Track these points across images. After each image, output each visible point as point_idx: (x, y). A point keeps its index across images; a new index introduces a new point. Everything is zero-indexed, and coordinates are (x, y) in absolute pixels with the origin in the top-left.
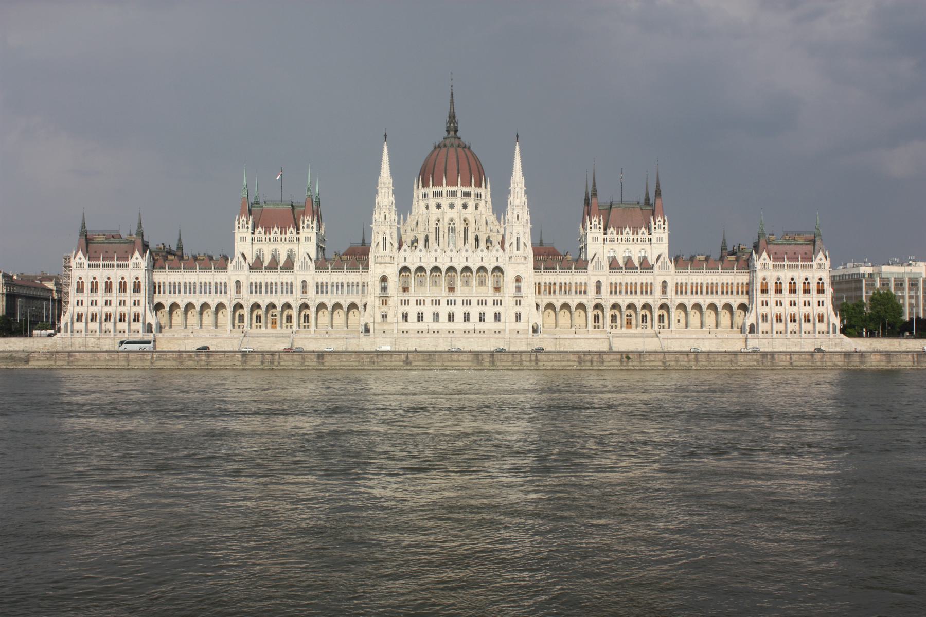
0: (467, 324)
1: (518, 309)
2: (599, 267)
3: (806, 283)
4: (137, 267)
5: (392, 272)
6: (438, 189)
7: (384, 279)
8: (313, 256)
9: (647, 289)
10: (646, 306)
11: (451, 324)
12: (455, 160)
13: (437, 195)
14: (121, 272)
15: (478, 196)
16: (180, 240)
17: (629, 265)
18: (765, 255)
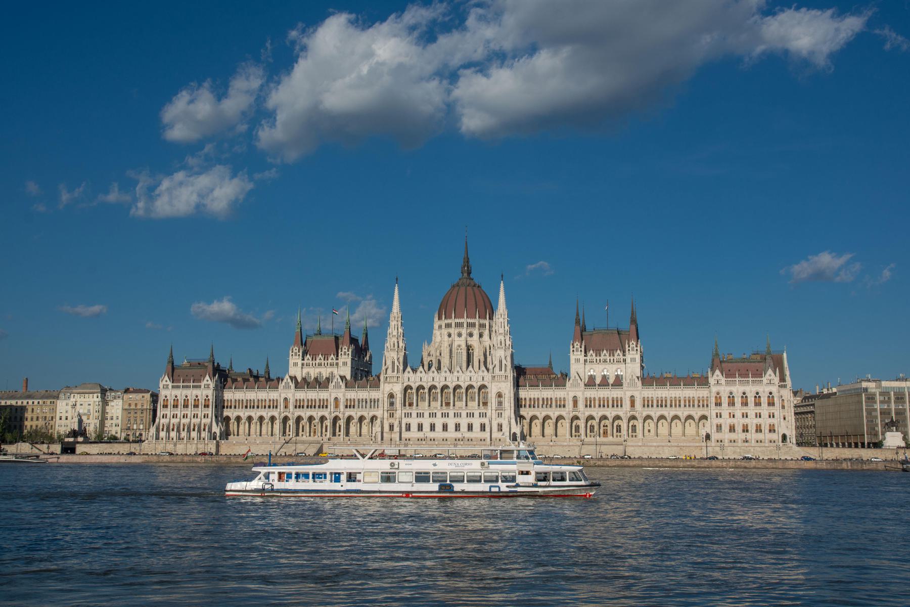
0: (457, 433)
1: (500, 420)
2: (576, 385)
3: (757, 396)
4: (206, 389)
5: (398, 389)
6: (449, 321)
7: (391, 396)
8: (348, 377)
9: (617, 403)
10: (618, 418)
11: (445, 433)
12: (464, 297)
13: (448, 326)
14: (196, 392)
15: (482, 326)
16: (267, 366)
17: (604, 383)
18: (718, 372)
